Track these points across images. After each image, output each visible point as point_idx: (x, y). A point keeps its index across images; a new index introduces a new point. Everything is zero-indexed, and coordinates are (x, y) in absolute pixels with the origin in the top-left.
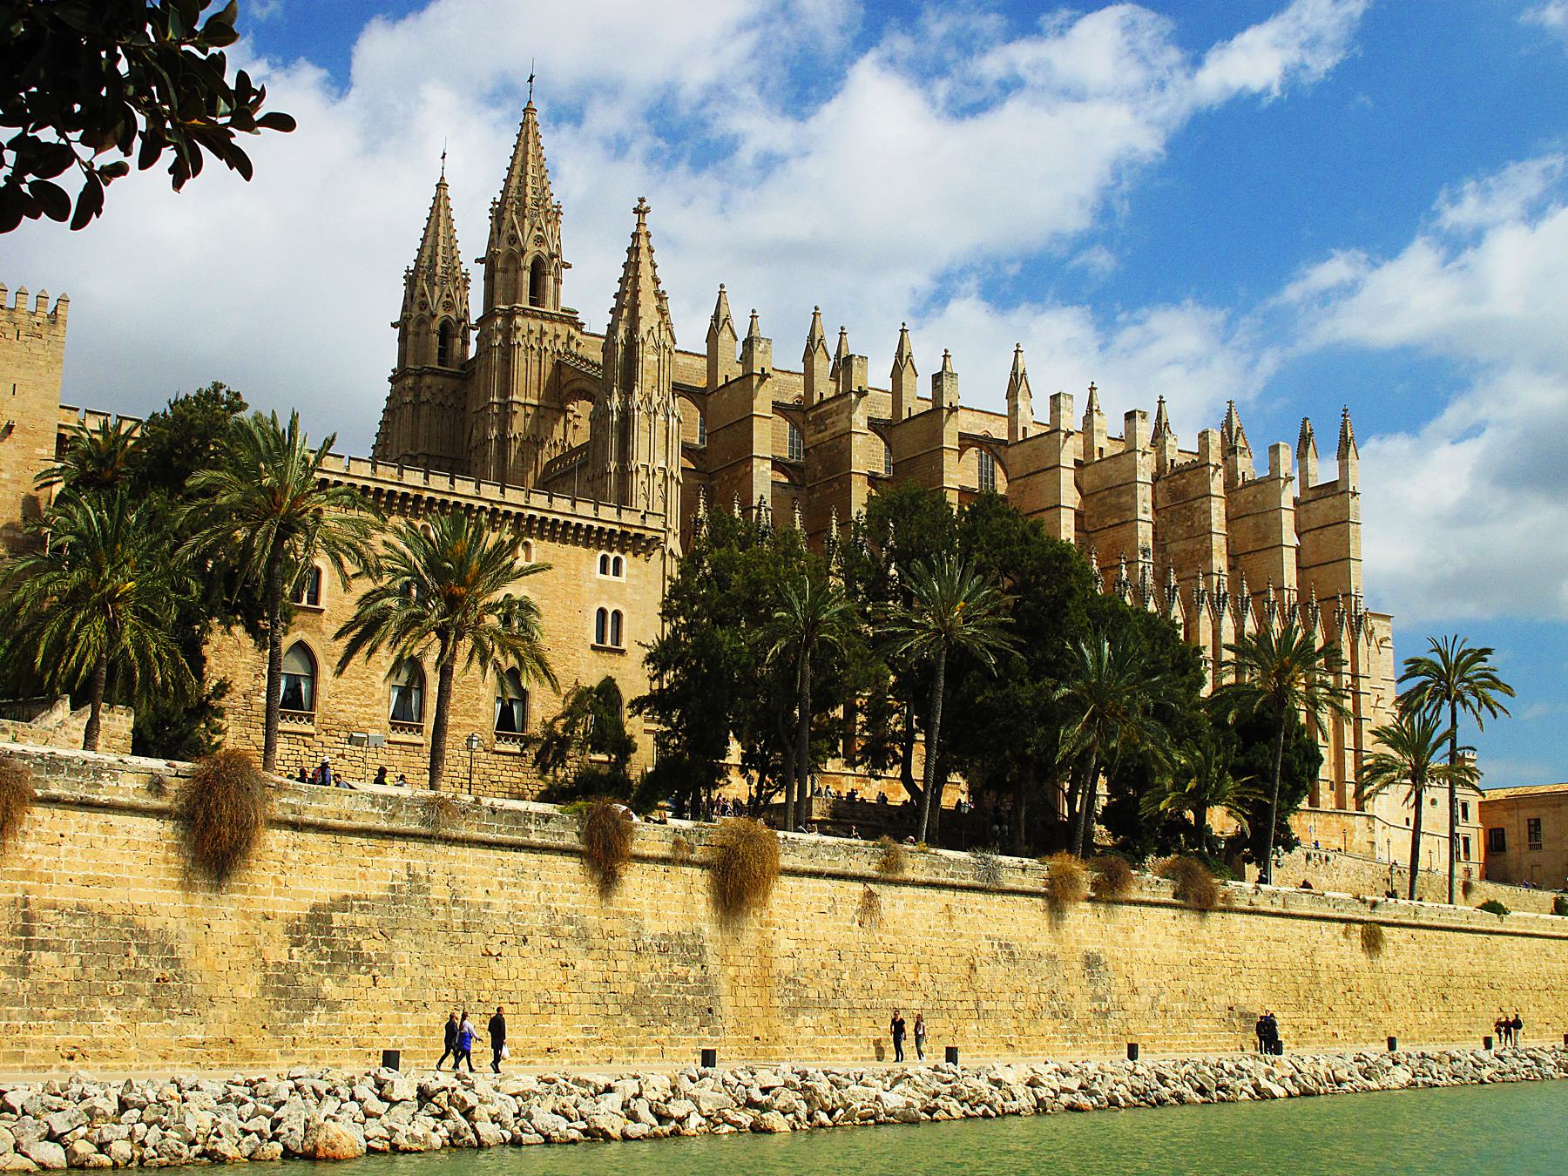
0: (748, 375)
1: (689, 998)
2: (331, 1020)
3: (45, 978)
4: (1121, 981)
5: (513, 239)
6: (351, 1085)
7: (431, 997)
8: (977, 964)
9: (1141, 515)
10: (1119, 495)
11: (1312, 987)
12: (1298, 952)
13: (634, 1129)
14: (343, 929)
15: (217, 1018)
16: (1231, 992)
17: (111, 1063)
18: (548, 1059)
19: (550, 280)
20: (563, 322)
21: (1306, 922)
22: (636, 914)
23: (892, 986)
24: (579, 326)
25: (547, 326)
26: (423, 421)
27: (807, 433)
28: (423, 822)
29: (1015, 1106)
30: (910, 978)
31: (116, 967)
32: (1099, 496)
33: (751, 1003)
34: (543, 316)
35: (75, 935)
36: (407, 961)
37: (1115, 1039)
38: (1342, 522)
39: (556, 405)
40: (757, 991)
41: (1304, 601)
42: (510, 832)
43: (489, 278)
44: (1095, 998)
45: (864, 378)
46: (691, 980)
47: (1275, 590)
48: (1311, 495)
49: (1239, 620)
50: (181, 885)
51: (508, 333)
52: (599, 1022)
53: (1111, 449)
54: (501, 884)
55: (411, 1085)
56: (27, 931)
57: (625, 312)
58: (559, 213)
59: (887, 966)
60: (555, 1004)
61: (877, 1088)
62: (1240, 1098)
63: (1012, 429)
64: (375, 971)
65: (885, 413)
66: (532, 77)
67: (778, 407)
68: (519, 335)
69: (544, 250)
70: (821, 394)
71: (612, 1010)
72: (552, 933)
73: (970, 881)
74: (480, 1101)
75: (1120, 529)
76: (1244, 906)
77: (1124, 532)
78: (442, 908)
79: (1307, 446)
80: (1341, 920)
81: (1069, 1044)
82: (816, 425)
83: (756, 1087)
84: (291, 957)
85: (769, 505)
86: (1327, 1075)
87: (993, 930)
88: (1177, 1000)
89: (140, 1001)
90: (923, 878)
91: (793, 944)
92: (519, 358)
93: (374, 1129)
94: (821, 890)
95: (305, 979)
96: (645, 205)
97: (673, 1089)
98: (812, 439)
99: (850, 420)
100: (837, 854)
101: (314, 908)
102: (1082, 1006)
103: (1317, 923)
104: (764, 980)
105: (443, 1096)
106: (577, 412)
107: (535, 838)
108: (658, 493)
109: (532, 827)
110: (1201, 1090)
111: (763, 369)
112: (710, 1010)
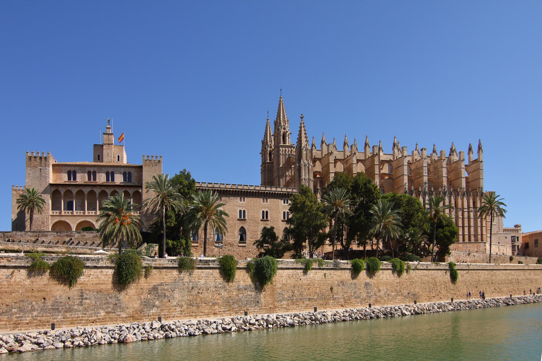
1: (252, 299)
2: (158, 310)
3: (87, 305)
4: (376, 288)
11: (434, 287)
12: (430, 278)
18: (214, 316)
36: (178, 296)
41: (467, 190)
46: (253, 295)
47: (460, 189)
54: (202, 277)
56: (82, 296)
59: (307, 289)
64: (169, 299)
72: (216, 287)
77: (421, 179)
78: (187, 283)
84: (148, 297)
91: (281, 285)
105: (167, 327)
107: (211, 266)
109: (210, 263)
112: (258, 302)
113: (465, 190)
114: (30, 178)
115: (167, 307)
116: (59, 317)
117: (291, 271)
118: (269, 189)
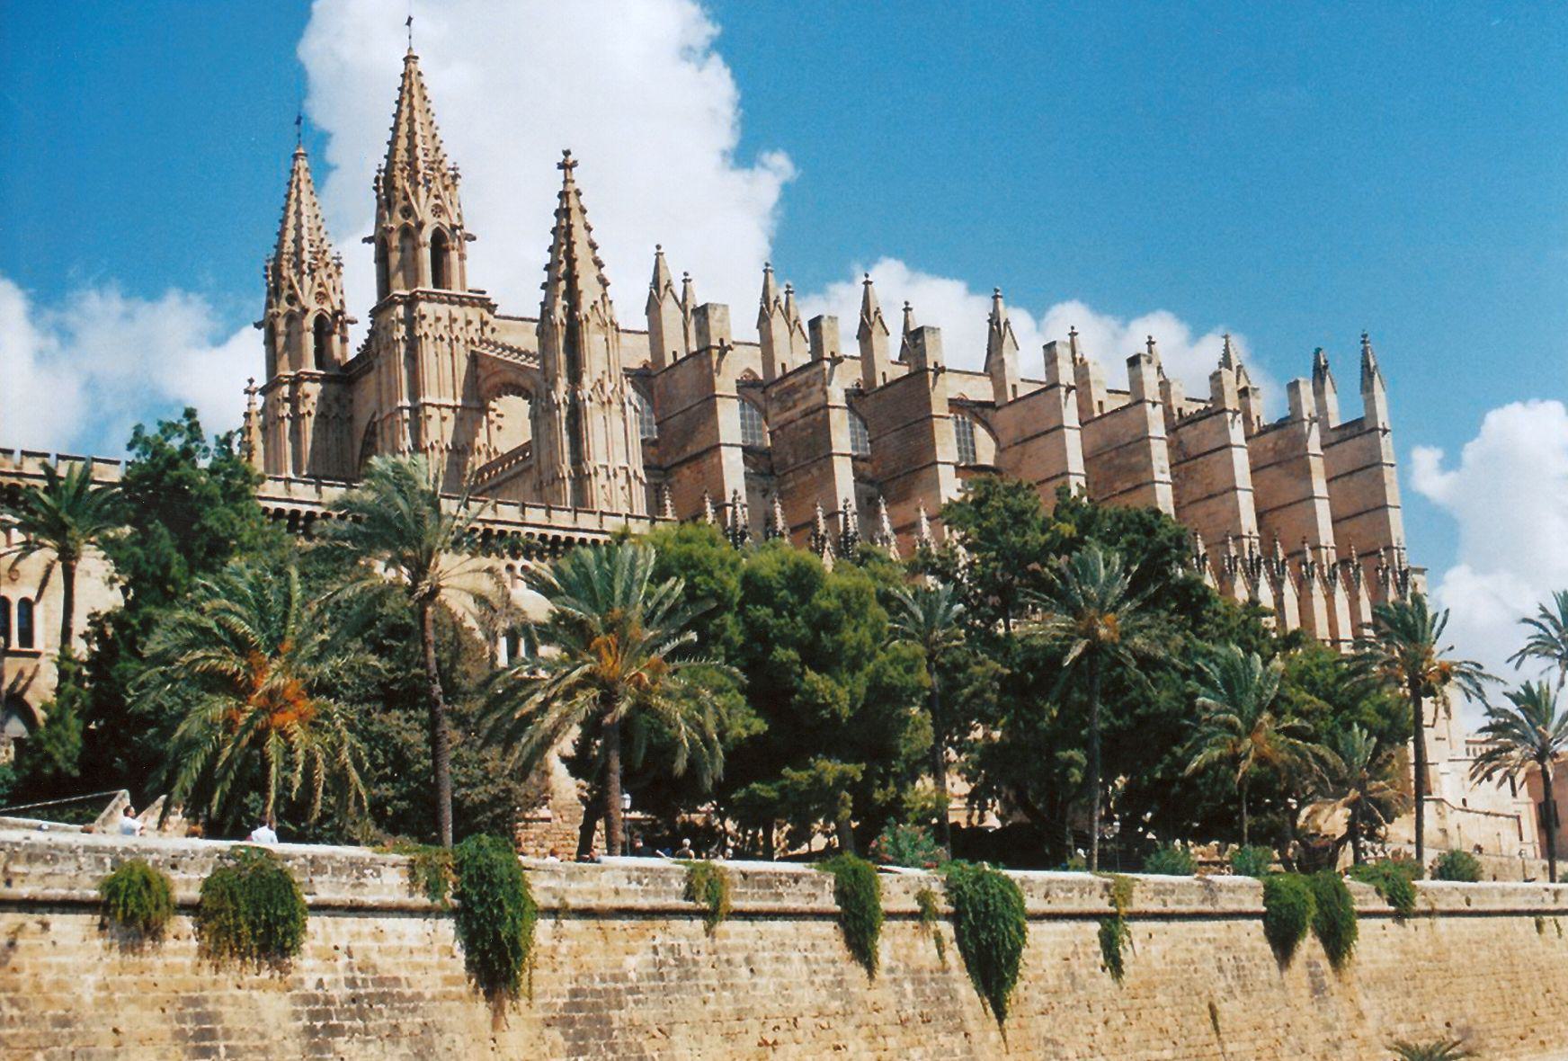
0: (705, 349)
9: (1158, 477)
10: (1132, 453)
14: (622, 1029)
19: (454, 255)
20: (474, 305)
24: (491, 308)
25: (457, 311)
27: (771, 413)
32: (1106, 457)
34: (450, 300)
39: (474, 404)
41: (1344, 562)
44: (1329, 1027)
45: (834, 343)
47: (1312, 549)
48: (1333, 437)
49: (1277, 584)
51: (411, 322)
53: (1112, 404)
57: (563, 285)
58: (455, 177)
63: (999, 388)
66: (410, 19)
68: (425, 323)
69: (445, 220)
70: (784, 366)
75: (1134, 494)
78: (712, 995)
79: (1323, 380)
80: (1530, 913)
82: (783, 402)
85: (744, 500)
88: (1400, 1020)
92: (428, 351)
96: (571, 159)
98: (776, 419)
99: (825, 393)
107: (789, 903)
108: (621, 497)
111: (721, 341)
113: (1333, 559)
118: (536, 515)
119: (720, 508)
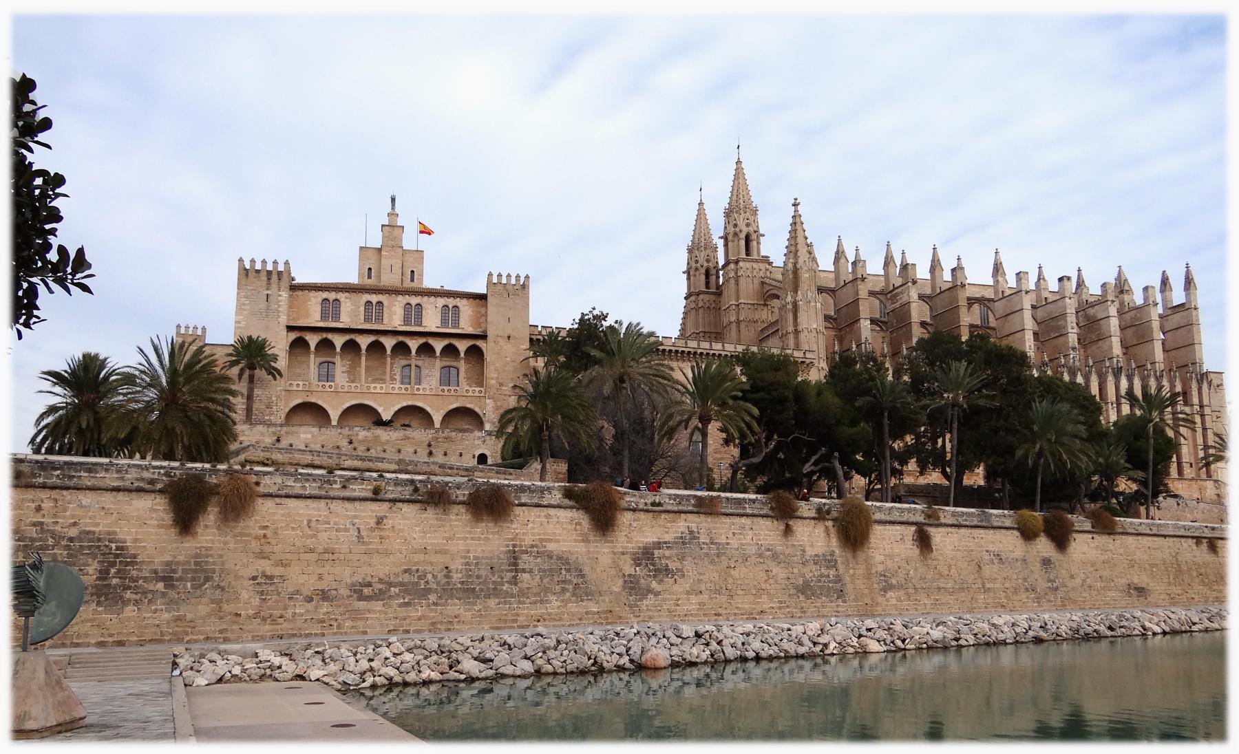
1: (831, 585)
5: (735, 226)
6: (664, 631)
7: (703, 588)
8: (982, 565)
9: (1070, 330)
10: (1058, 320)
13: (802, 650)
15: (604, 601)
16: (1129, 576)
17: (557, 623)
19: (755, 243)
21: (1172, 539)
22: (801, 545)
23: (937, 577)
24: (770, 263)
25: (755, 265)
26: (701, 315)
28: (694, 506)
29: (1001, 637)
30: (947, 572)
31: (556, 579)
33: (862, 587)
34: (753, 261)
35: (537, 565)
37: (1062, 602)
38: (1189, 326)
40: (865, 581)
42: (736, 508)
43: (726, 245)
44: (1050, 581)
48: (1169, 312)
49: (1130, 379)
50: (583, 541)
52: (786, 598)
54: (734, 534)
55: (691, 631)
56: (516, 564)
58: (757, 210)
60: (764, 590)
61: (927, 628)
62: (1134, 633)
63: (996, 292)
64: (676, 577)
65: (928, 291)
67: (872, 293)
69: (751, 229)
71: (793, 591)
72: (760, 556)
73: (975, 523)
74: (725, 637)
75: (1060, 338)
76: (1133, 531)
77: (1061, 340)
79: (1165, 285)
80: (1193, 537)
81: (1035, 605)
83: (864, 628)
84: (636, 571)
86: (1186, 620)
87: (990, 548)
89: (568, 594)
90: (951, 523)
91: (882, 558)
92: (742, 281)
93: (675, 651)
94: (897, 531)
95: (643, 581)
96: (798, 201)
97: (822, 630)
99: (908, 295)
100: (903, 512)
101: (645, 548)
102: (1042, 585)
103: (1178, 539)
104: (868, 575)
105: (707, 635)
106: (773, 305)
107: (749, 511)
109: (747, 506)
110: (1110, 628)
112: (841, 591)
113: (1162, 367)
114: (246, 312)
115: (672, 593)
116: (475, 607)
117: (898, 527)
119: (858, 346)
